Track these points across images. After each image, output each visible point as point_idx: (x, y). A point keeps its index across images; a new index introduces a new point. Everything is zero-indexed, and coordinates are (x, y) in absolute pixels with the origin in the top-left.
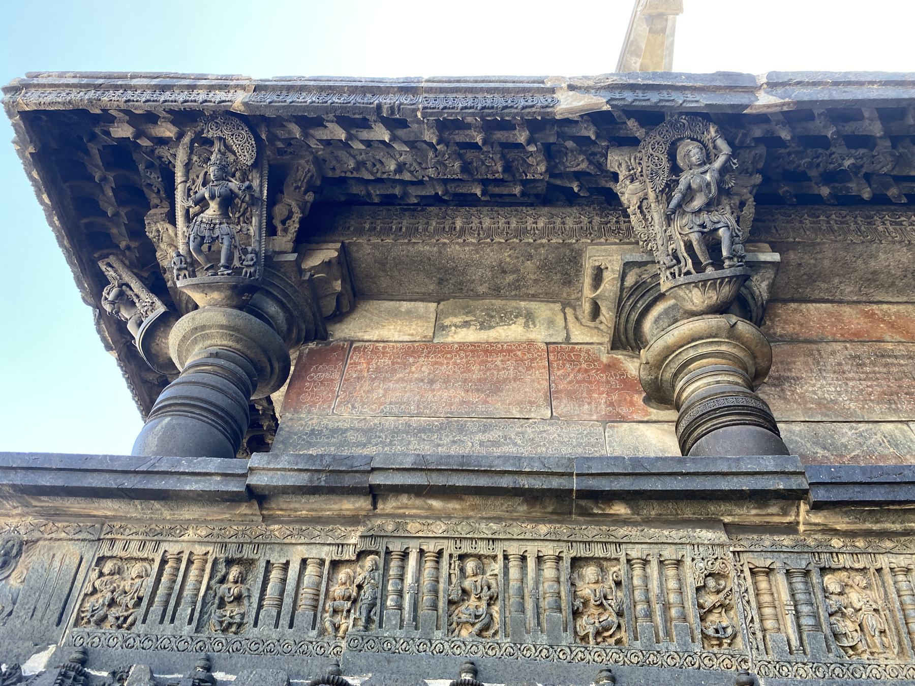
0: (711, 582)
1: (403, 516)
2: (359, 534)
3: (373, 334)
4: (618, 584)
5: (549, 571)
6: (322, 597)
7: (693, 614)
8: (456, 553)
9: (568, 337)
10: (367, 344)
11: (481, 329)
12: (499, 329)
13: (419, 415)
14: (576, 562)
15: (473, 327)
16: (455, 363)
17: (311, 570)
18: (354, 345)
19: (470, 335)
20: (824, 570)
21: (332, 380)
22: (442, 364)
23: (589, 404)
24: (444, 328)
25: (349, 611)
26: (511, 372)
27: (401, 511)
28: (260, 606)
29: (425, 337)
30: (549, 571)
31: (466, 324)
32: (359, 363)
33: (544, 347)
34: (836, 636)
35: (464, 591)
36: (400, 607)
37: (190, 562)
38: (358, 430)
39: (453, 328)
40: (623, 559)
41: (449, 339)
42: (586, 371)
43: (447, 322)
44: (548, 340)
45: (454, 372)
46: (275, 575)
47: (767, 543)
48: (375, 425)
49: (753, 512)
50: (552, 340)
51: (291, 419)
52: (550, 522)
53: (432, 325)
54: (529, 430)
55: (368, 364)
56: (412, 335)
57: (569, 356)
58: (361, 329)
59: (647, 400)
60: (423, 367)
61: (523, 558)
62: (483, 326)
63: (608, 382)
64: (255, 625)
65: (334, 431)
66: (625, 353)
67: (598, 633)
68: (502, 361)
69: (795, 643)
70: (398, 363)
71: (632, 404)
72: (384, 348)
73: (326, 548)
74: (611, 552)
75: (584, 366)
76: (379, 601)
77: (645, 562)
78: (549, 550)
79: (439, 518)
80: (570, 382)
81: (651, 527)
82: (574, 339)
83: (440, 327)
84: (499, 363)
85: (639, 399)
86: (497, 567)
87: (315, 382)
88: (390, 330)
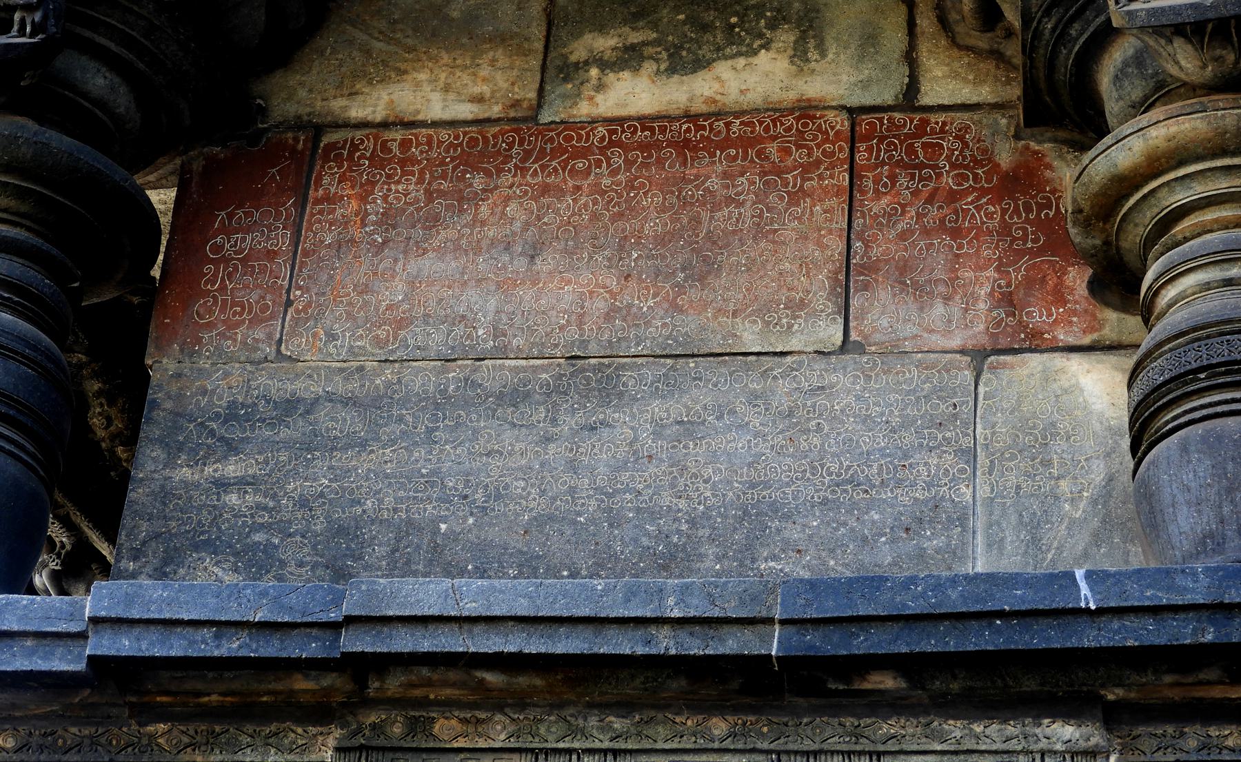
1: (424, 703)
2: (331, 742)
3: (372, 104)
9: (912, 88)
10: (359, 134)
11: (672, 70)
12: (723, 69)
13: (502, 353)
15: (649, 67)
16: (598, 190)
18: (326, 140)
19: (635, 94)
21: (271, 255)
22: (560, 193)
23: (947, 299)
24: (570, 71)
26: (747, 211)
27: (418, 693)
29: (516, 104)
31: (630, 58)
32: (340, 204)
33: (841, 122)
38: (348, 401)
39: (594, 72)
41: (584, 110)
42: (953, 197)
43: (578, 51)
44: (855, 101)
45: (595, 217)
47: (1192, 743)
48: (389, 384)
49: (1168, 679)
50: (868, 100)
51: (178, 376)
52: (736, 710)
53: (535, 63)
54: (784, 386)
55: (363, 199)
56: (479, 99)
57: (911, 150)
58: (340, 86)
59: (1097, 288)
60: (509, 207)
62: (682, 61)
63: (1005, 230)
65: (290, 406)
66: (1062, 134)
68: (725, 175)
70: (442, 194)
71: (1059, 297)
72: (405, 145)
75: (948, 181)
79: (500, 708)
80: (903, 236)
81: (948, 717)
82: (926, 99)
83: (558, 70)
84: (714, 183)
85: (1077, 279)
87: (226, 260)
88: (418, 85)
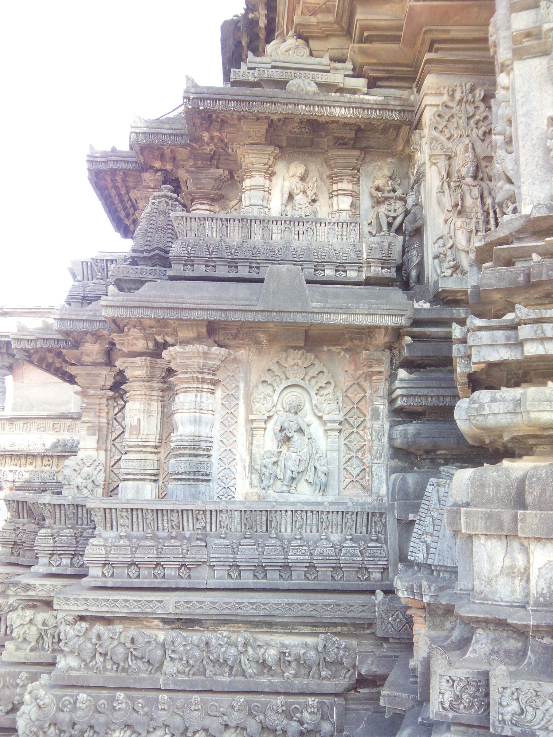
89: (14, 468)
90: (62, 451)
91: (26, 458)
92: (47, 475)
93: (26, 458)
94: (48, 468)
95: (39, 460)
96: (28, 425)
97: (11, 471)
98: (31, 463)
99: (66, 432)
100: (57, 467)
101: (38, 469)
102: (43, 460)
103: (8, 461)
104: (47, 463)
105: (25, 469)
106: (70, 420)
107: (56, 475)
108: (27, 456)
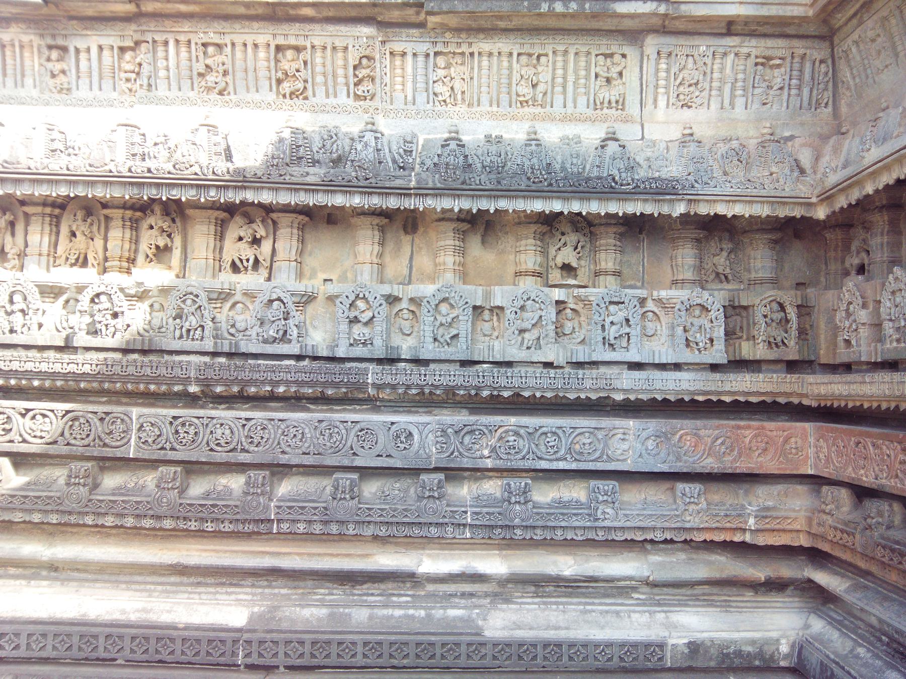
0: (364, 61)
4: (305, 63)
5: (262, 54)
6: (117, 71)
7: (352, 80)
8: (200, 42)
14: (278, 48)
17: (106, 53)
20: (436, 54)
25: (135, 80)
28: (79, 77)
30: (262, 54)
34: (435, 94)
35: (207, 66)
36: (168, 78)
37: (22, 47)
40: (309, 46)
46: (83, 56)
61: (245, 45)
64: (78, 89)
67: (292, 94)
69: (410, 98)
73: (113, 38)
74: (301, 42)
76: (153, 74)
77: (325, 48)
78: (261, 39)
86: (228, 49)
89: (66, 276)
90: (329, 186)
91: (135, 225)
92: (243, 318)
93: (135, 225)
94: (248, 280)
95: (201, 239)
96: (143, 54)
97: (51, 292)
98: (161, 253)
99: (343, 99)
100: (300, 275)
101: (199, 278)
102: (220, 236)
103: (38, 237)
104: (247, 252)
105: (128, 282)
106: (366, 30)
107: (297, 317)
108: (139, 210)
